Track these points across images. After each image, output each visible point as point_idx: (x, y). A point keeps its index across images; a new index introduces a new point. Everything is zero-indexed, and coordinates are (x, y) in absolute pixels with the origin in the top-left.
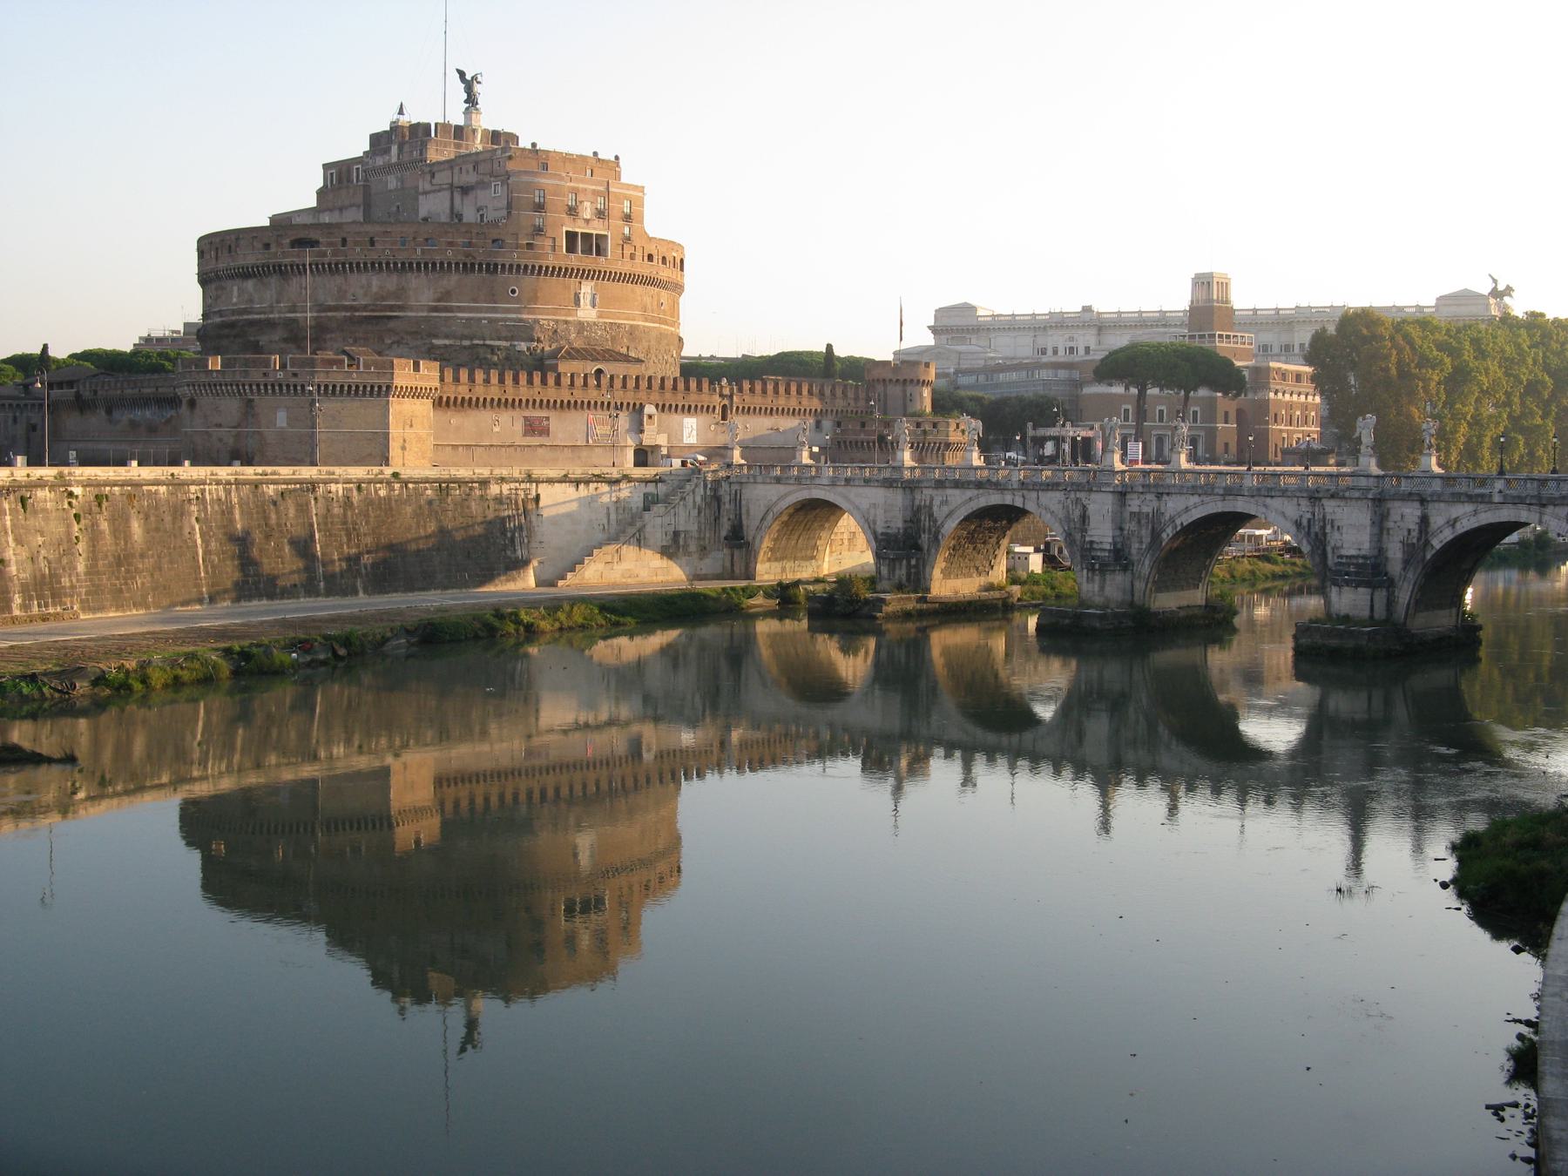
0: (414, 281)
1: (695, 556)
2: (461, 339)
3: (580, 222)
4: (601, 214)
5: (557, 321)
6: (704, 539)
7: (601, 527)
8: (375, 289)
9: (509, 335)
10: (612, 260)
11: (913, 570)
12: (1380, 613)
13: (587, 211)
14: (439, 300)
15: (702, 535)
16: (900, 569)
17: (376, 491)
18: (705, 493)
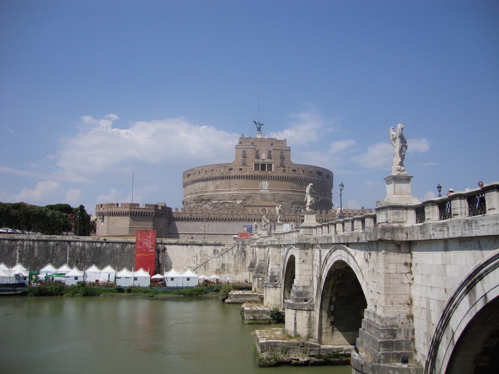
0: (210, 183)
1: (233, 274)
2: (220, 201)
4: (270, 157)
5: (252, 193)
6: (237, 267)
7: (194, 261)
8: (201, 187)
9: (235, 198)
10: (275, 171)
11: (260, 283)
12: (303, 330)
13: (264, 156)
15: (236, 266)
16: (255, 282)
17: (96, 245)
18: (238, 249)
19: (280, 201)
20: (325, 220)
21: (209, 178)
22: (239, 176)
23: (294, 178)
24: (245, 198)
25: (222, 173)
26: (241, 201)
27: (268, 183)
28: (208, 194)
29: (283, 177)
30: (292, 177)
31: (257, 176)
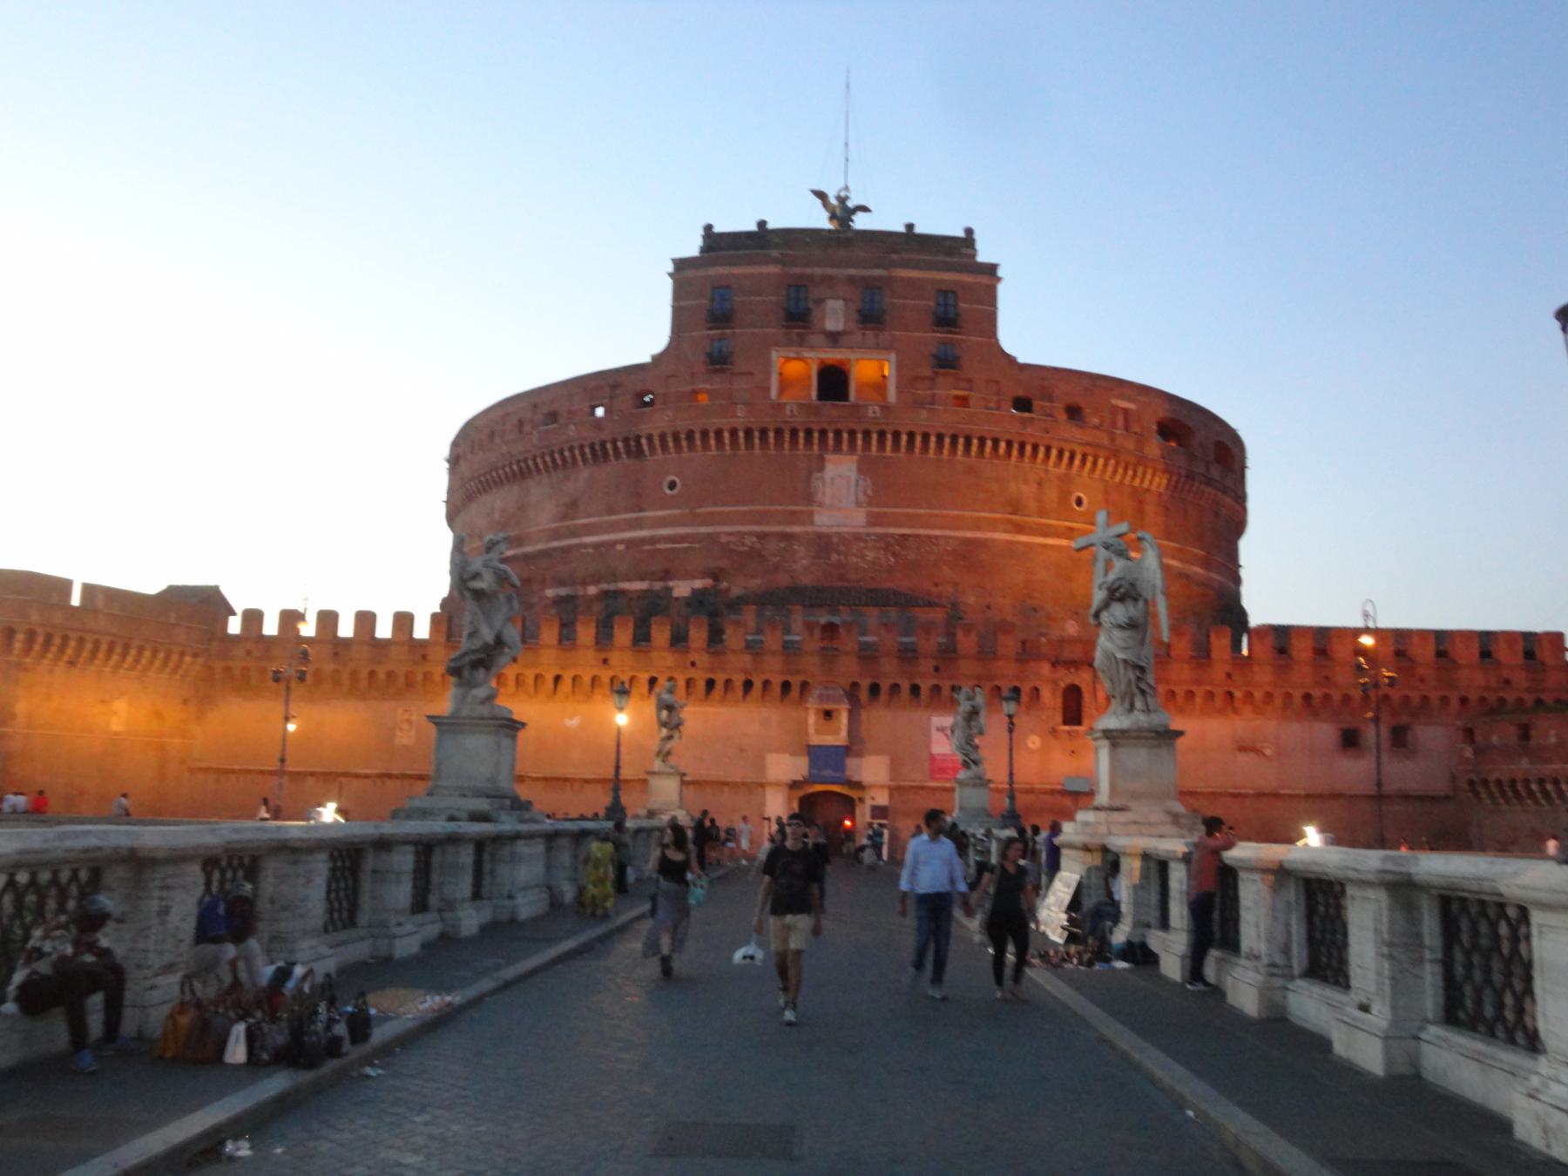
0: (538, 489)
2: (585, 583)
3: (817, 339)
4: (870, 318)
5: (762, 536)
8: (497, 516)
13: (834, 316)
14: (564, 517)
19: (936, 585)
20: (1230, 694)
21: (534, 459)
22: (690, 435)
23: (1022, 446)
24: (723, 563)
25: (598, 424)
26: (698, 584)
27: (860, 471)
28: (529, 549)
29: (954, 438)
30: (1009, 444)
31: (794, 432)
